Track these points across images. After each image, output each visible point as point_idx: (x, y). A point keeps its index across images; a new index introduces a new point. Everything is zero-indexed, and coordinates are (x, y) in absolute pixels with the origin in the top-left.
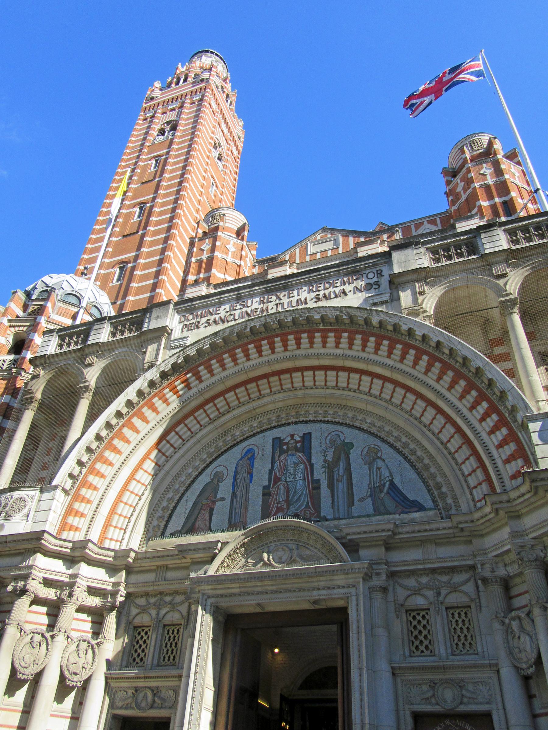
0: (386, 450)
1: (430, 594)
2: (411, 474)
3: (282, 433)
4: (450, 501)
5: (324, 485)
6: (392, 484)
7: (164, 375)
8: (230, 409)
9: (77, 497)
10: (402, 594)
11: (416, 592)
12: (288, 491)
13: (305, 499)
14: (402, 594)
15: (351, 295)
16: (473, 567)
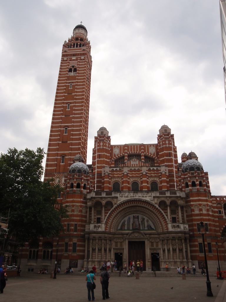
0: (150, 221)
1: (154, 240)
2: (152, 224)
3: (134, 215)
4: (157, 229)
5: (141, 224)
6: (150, 226)
7: (118, 206)
10: (151, 240)
11: (152, 240)
12: (136, 224)
14: (151, 240)
15: (147, 197)
16: (159, 238)
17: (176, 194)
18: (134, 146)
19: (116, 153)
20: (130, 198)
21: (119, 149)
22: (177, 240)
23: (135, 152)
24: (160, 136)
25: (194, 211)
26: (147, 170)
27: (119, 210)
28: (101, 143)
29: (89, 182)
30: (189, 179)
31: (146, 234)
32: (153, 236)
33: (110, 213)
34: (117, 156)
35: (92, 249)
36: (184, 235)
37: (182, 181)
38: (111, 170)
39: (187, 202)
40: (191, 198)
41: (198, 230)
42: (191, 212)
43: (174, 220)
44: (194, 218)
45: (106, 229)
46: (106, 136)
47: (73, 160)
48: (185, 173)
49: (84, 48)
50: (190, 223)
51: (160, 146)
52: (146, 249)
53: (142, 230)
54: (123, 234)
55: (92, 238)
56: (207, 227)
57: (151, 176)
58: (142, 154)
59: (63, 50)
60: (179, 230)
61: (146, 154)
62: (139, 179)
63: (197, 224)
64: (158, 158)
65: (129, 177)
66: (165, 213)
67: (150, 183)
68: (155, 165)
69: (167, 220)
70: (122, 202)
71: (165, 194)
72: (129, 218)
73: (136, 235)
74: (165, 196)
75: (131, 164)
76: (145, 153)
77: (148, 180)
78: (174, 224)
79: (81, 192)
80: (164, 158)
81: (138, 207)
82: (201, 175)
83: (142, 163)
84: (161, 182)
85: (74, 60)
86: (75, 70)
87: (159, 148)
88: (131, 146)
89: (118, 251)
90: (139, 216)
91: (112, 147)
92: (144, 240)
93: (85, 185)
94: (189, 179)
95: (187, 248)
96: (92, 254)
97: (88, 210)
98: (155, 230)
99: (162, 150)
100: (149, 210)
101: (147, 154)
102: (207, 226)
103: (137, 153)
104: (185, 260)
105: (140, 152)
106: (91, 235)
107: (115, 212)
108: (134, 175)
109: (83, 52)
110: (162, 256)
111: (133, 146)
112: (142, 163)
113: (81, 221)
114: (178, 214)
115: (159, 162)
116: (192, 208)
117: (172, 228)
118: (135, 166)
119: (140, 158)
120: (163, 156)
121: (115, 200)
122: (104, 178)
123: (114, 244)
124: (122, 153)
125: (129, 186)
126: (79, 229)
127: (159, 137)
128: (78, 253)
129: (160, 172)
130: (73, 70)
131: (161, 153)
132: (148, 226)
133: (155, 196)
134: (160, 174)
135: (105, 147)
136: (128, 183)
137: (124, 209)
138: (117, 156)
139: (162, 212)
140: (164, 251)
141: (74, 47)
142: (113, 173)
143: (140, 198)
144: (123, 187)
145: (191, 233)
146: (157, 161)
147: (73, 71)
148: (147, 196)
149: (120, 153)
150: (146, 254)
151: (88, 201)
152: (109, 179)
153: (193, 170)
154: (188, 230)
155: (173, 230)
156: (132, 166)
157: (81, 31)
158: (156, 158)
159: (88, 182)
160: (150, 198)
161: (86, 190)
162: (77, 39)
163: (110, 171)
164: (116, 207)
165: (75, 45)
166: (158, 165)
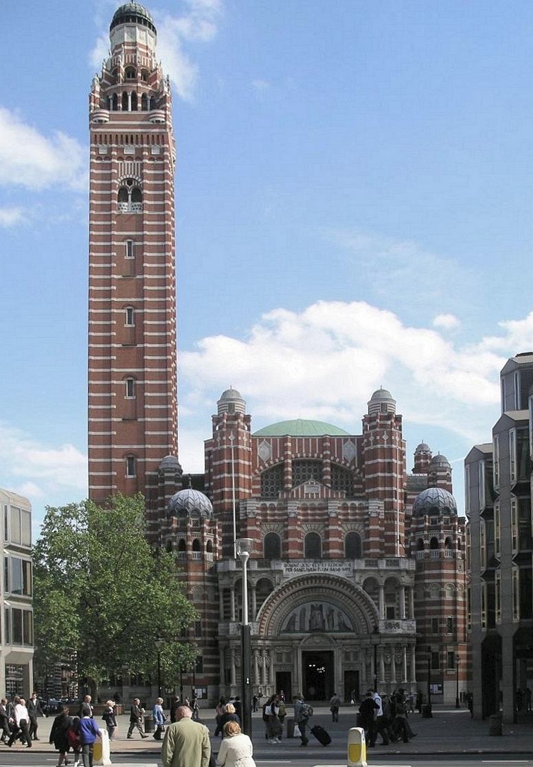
2: (348, 620)
3: (313, 603)
5: (326, 621)
6: (344, 623)
7: (283, 587)
8: (299, 595)
9: (261, 624)
11: (347, 649)
13: (321, 625)
15: (342, 571)
17: (398, 565)
18: (307, 440)
19: (264, 458)
20: (307, 573)
21: (271, 446)
22: (393, 650)
23: (310, 455)
24: (370, 418)
25: (429, 597)
26: (339, 508)
27: (285, 595)
28: (230, 435)
29: (217, 536)
30: (426, 533)
31: (335, 639)
32: (348, 641)
33: (267, 602)
34: (267, 465)
35: (236, 667)
36: (406, 640)
37: (412, 535)
38: (259, 506)
39: (417, 578)
40: (427, 572)
41: (434, 629)
42: (425, 596)
43: (391, 614)
44: (428, 608)
45: (260, 632)
46: (242, 415)
47: (157, 470)
48: (420, 519)
49: (160, 115)
50: (419, 618)
51: (368, 444)
52: (335, 666)
53: (329, 631)
54: (291, 639)
55: (234, 647)
56: (451, 626)
57: (347, 520)
58: (325, 461)
59: (91, 117)
60: (400, 631)
61: (334, 460)
62: (322, 526)
63: (433, 619)
64: (364, 471)
65: (299, 523)
66: (373, 599)
67: (344, 536)
68: (355, 486)
69: (378, 613)
70: (292, 581)
71: (377, 565)
72: (304, 610)
73: (318, 641)
74: (376, 568)
75: (305, 492)
76: (332, 458)
77: (340, 529)
78: (391, 621)
79: (203, 557)
80: (375, 475)
81: (321, 589)
82: (450, 525)
83: (330, 491)
84: (368, 534)
85: (130, 157)
86: (138, 195)
87: (366, 449)
88: (300, 440)
89: (283, 670)
90: (324, 606)
91: (255, 440)
92: (332, 649)
93: (209, 541)
94: (426, 533)
95: (409, 662)
96: (236, 676)
97: (221, 594)
98: (354, 632)
99: (374, 454)
100: (343, 594)
101: (338, 460)
102: (451, 622)
103: (313, 456)
104: (406, 681)
105: (321, 456)
106: (231, 641)
107: (277, 598)
108: (310, 518)
109: (157, 130)
110: (364, 675)
111: (305, 439)
112: (330, 491)
113: (210, 616)
114: (398, 601)
115: (364, 480)
116: (427, 590)
117: (387, 628)
118: (312, 497)
119: (321, 470)
120: (374, 468)
121: (277, 577)
122: (245, 523)
123: (273, 657)
124: (278, 456)
125: (299, 541)
126: (205, 632)
127: (368, 420)
128: (206, 675)
129: (366, 511)
130: (130, 192)
131: (370, 462)
132: (339, 625)
133: (356, 568)
134: (366, 517)
135: (240, 447)
136: (298, 534)
137: (294, 593)
138: (267, 465)
139: (370, 599)
140: (368, 666)
141: (125, 108)
142: (264, 512)
143: (327, 572)
144: (287, 543)
145: (421, 636)
146: (360, 477)
147: (130, 196)
148: (341, 568)
149: (275, 456)
150: (335, 672)
151: (220, 577)
152: (257, 526)
153: (437, 514)
154: (414, 632)
155: (388, 631)
156: (307, 497)
157: (142, 35)
158: (358, 470)
159: (215, 536)
160: (347, 571)
161: (211, 554)
162: (131, 72)
163: (258, 508)
164: (279, 590)
165: (130, 98)
166: (361, 486)
